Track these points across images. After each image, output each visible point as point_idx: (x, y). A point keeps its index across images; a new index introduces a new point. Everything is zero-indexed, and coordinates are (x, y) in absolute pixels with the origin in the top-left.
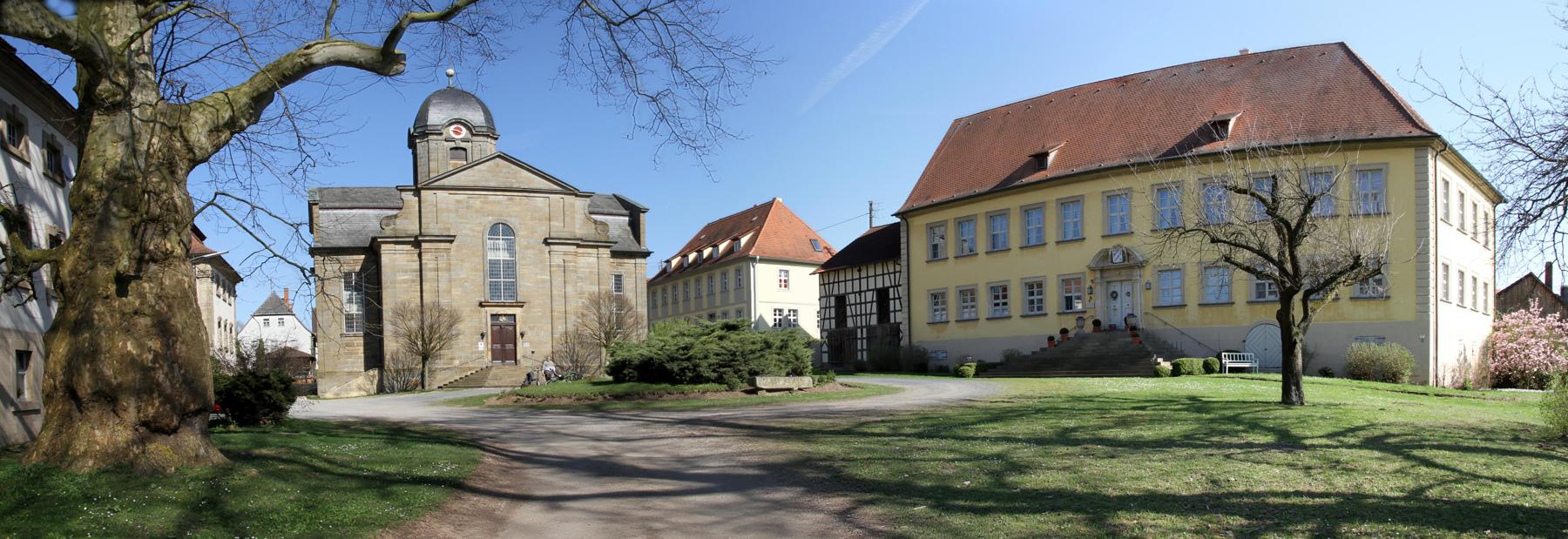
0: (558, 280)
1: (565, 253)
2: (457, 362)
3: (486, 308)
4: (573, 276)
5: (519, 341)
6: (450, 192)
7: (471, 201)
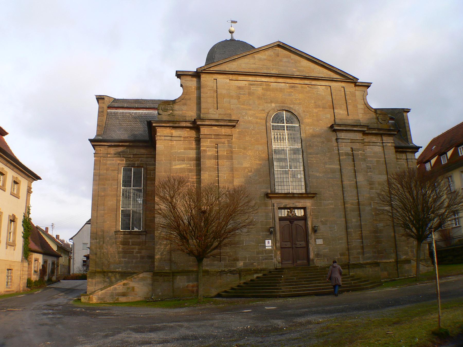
0: (348, 169)
1: (353, 141)
2: (240, 264)
3: (274, 201)
4: (363, 165)
5: (312, 237)
6: (231, 77)
7: (253, 88)
